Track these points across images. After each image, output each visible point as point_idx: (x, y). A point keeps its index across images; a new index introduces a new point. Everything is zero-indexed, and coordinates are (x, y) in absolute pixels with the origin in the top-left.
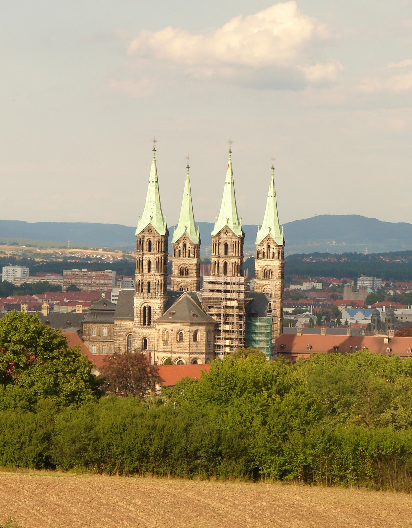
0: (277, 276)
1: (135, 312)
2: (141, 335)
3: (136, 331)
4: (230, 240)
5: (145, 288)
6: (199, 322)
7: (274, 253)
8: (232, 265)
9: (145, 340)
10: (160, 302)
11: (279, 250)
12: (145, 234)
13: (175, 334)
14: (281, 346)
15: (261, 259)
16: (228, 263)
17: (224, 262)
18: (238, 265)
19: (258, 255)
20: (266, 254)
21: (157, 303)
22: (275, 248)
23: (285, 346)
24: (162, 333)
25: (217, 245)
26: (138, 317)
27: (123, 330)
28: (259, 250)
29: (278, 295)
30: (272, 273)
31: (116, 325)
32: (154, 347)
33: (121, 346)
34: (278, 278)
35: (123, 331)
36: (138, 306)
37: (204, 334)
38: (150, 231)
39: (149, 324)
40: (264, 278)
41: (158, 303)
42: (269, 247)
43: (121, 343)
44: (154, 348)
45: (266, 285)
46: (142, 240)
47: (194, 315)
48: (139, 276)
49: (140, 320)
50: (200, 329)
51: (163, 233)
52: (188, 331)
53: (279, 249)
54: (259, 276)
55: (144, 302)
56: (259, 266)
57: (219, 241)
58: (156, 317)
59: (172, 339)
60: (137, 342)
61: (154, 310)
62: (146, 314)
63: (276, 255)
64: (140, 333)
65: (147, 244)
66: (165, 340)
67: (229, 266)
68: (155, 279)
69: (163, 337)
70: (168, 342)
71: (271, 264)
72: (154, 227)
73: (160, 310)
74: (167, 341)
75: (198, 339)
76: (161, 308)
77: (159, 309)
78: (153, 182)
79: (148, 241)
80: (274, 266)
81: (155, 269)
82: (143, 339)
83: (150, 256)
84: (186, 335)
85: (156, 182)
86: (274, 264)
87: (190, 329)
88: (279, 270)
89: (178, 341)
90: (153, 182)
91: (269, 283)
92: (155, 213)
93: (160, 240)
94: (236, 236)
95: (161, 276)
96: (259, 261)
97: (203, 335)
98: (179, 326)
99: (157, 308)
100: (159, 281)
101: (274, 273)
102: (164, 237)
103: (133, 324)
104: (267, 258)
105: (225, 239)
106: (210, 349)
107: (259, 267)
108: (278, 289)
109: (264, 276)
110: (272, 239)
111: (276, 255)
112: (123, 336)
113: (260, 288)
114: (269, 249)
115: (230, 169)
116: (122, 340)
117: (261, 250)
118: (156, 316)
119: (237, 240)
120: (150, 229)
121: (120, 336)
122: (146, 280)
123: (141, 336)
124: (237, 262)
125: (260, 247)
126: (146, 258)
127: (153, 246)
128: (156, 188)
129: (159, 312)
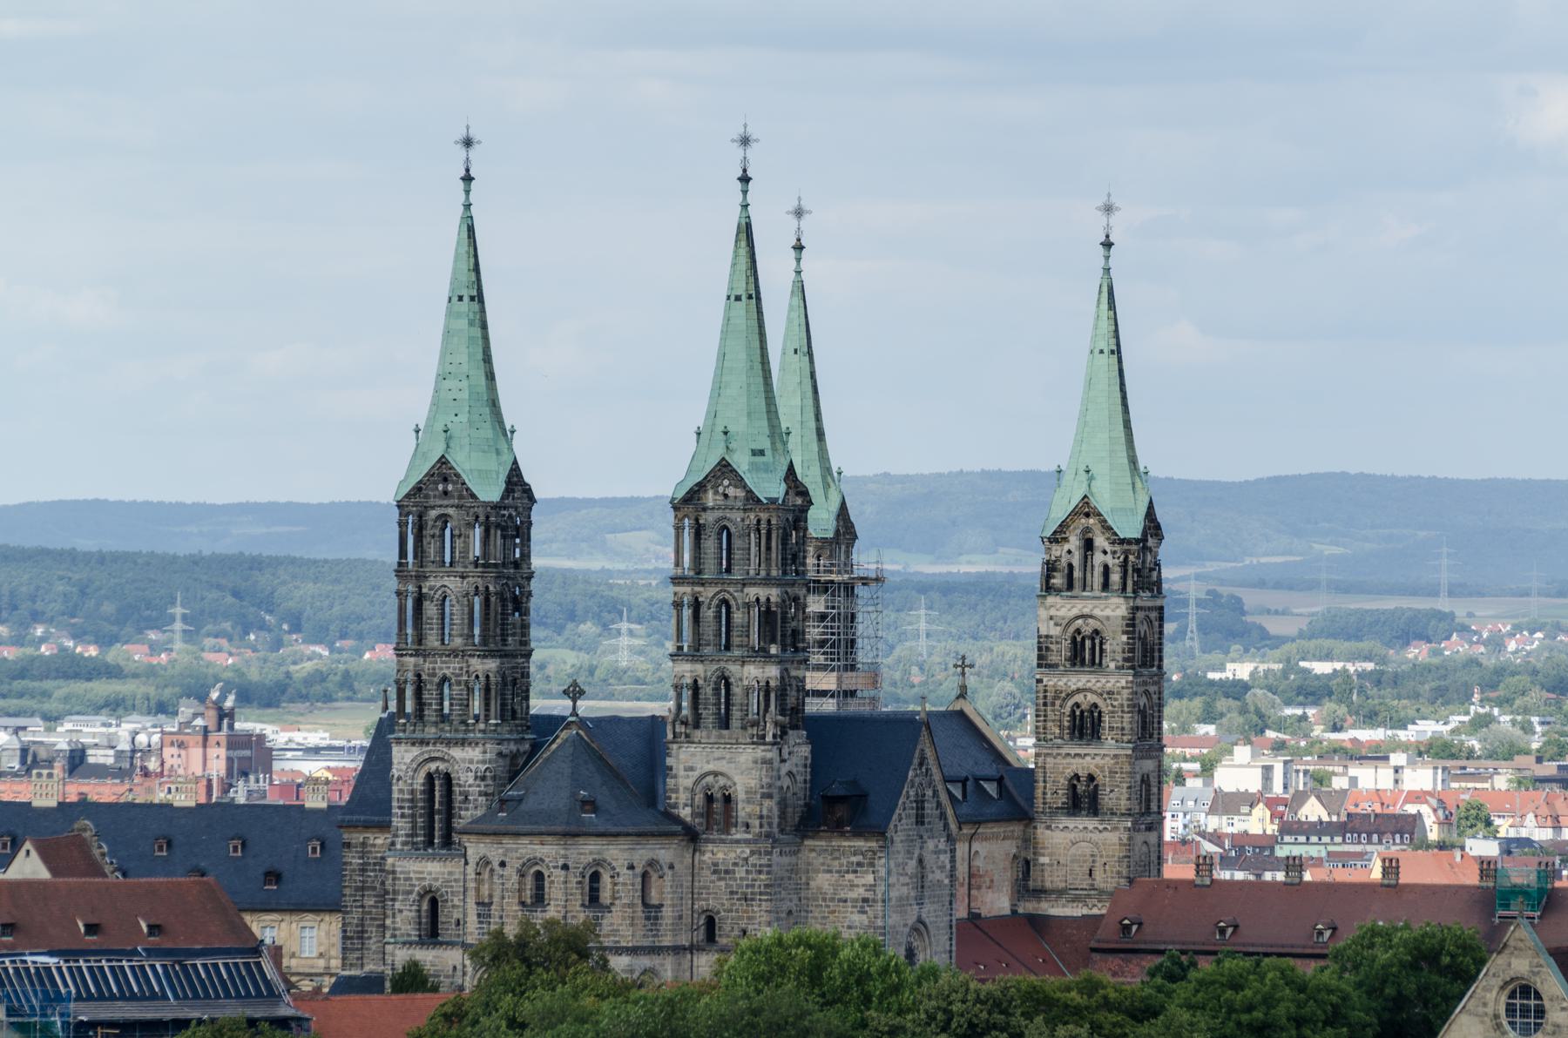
0: (1120, 659)
1: (395, 795)
2: (414, 882)
3: (398, 869)
4: (737, 516)
5: (431, 704)
6: (601, 829)
7: (1106, 570)
8: (746, 610)
9: (434, 903)
10: (481, 757)
11: (1126, 559)
12: (427, 496)
13: (515, 878)
14: (1120, 923)
15: (1058, 591)
16: (732, 603)
17: (715, 602)
18: (768, 608)
19: (1048, 577)
20: (1077, 574)
21: (471, 761)
22: (1108, 548)
23: (1140, 924)
24: (473, 876)
26: (403, 816)
27: (375, 864)
28: (1053, 558)
29: (1123, 729)
30: (1101, 644)
31: (348, 845)
32: (461, 927)
33: (370, 925)
34: (1120, 664)
35: (375, 870)
36: (402, 774)
37: (625, 876)
39: (447, 842)
40: (1074, 665)
41: (476, 759)
42: (1088, 545)
43: (370, 913)
44: (461, 932)
45: (1078, 691)
47: (590, 805)
48: (407, 659)
49: (414, 828)
50: (609, 860)
51: (490, 491)
52: (560, 864)
53: (1126, 553)
54: (1053, 658)
55: (426, 756)
56: (1051, 618)
57: (697, 520)
58: (469, 813)
59: (503, 898)
60: (401, 911)
61: (460, 786)
62: (434, 802)
63: (1115, 577)
64: (412, 875)
65: (433, 536)
66: (486, 901)
67: (738, 617)
68: (465, 669)
69: (478, 890)
70: (493, 907)
71: (1097, 612)
72: (459, 470)
73: (482, 788)
74: (491, 904)
75: (605, 896)
76: (483, 778)
77: (478, 782)
78: (461, 298)
79: (439, 523)
80: (1108, 618)
81: (466, 632)
82: (421, 896)
83: (447, 581)
84: (553, 882)
85: (472, 299)
86: (1108, 612)
87: (565, 857)
88: (1124, 632)
89: (523, 904)
90: (461, 298)
91: (1089, 685)
92: (463, 418)
93: (482, 518)
94: (759, 501)
95: (485, 657)
96: (1051, 600)
97: (621, 879)
98: (528, 848)
99: (471, 781)
100: (477, 677)
101: (1107, 647)
102: (496, 507)
103: (389, 840)
104: (1084, 590)
105: (718, 514)
106: (654, 936)
107: (1052, 623)
108: (1122, 705)
109: (1075, 657)
110: (1099, 514)
111: (1115, 577)
112: (374, 888)
113: (1058, 703)
114: (1090, 553)
115: (743, 244)
116: (369, 902)
117: (1058, 559)
118: (467, 809)
119: (764, 516)
121: (363, 889)
122: (434, 675)
123: (417, 889)
124: (763, 599)
125: (1055, 547)
126: (431, 588)
128: (471, 323)
129: (480, 795)
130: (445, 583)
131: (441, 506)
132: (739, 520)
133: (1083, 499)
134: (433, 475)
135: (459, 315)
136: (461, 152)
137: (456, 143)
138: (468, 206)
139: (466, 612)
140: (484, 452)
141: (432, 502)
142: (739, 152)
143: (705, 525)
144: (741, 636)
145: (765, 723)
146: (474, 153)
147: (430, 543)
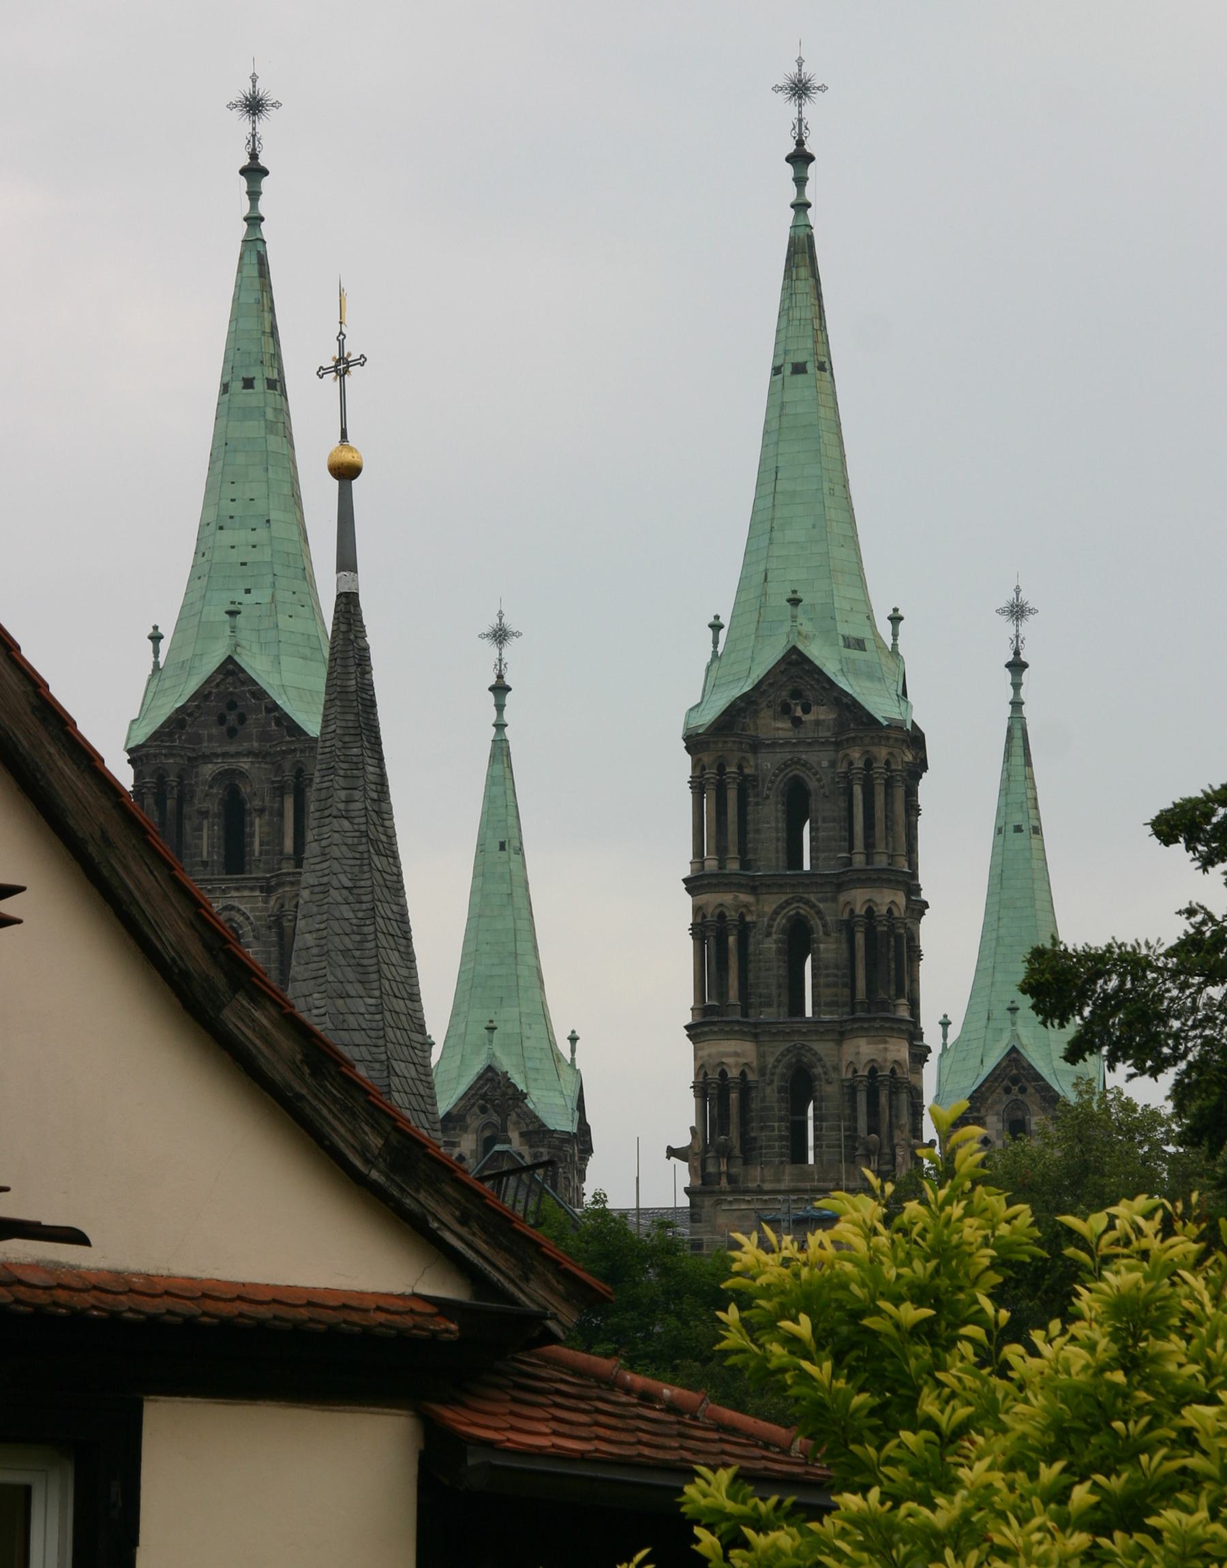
4: (821, 759)
16: (816, 923)
17: (781, 921)
25: (732, 795)
38: (232, 718)
46: (172, 779)
78: (248, 383)
105: (782, 756)
120: (232, 706)
127: (258, 828)
130: (236, 903)
131: (225, 755)
132: (825, 764)
133: (1008, 1054)
134: (207, 697)
135: (246, 413)
136: (241, 124)
137: (232, 106)
138: (254, 220)
139: (274, 956)
140: (304, 658)
141: (206, 747)
142: (788, 109)
143: (755, 778)
144: (835, 985)
145: (893, 1148)
146: (267, 125)
147: (199, 828)
